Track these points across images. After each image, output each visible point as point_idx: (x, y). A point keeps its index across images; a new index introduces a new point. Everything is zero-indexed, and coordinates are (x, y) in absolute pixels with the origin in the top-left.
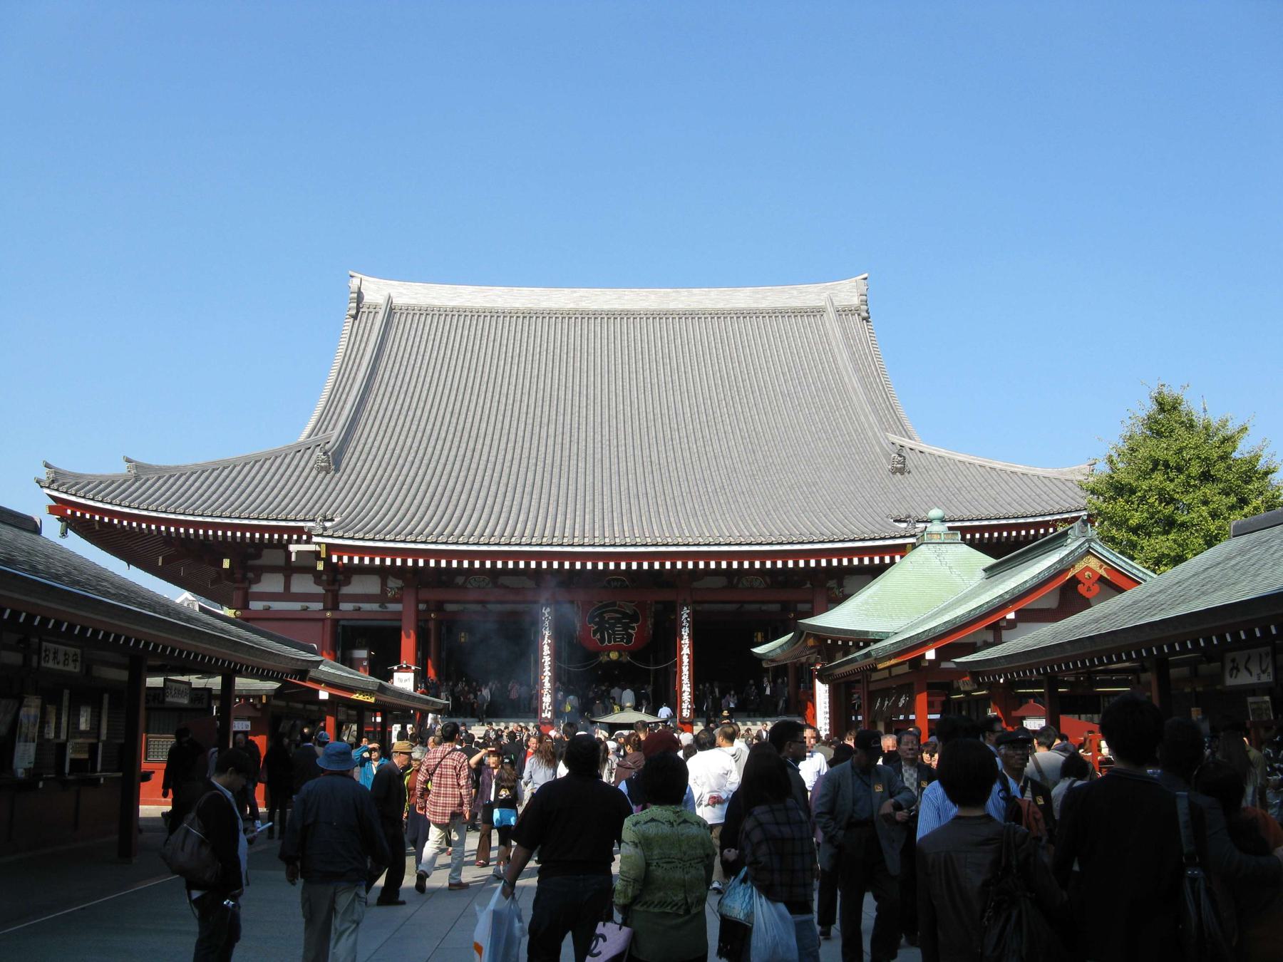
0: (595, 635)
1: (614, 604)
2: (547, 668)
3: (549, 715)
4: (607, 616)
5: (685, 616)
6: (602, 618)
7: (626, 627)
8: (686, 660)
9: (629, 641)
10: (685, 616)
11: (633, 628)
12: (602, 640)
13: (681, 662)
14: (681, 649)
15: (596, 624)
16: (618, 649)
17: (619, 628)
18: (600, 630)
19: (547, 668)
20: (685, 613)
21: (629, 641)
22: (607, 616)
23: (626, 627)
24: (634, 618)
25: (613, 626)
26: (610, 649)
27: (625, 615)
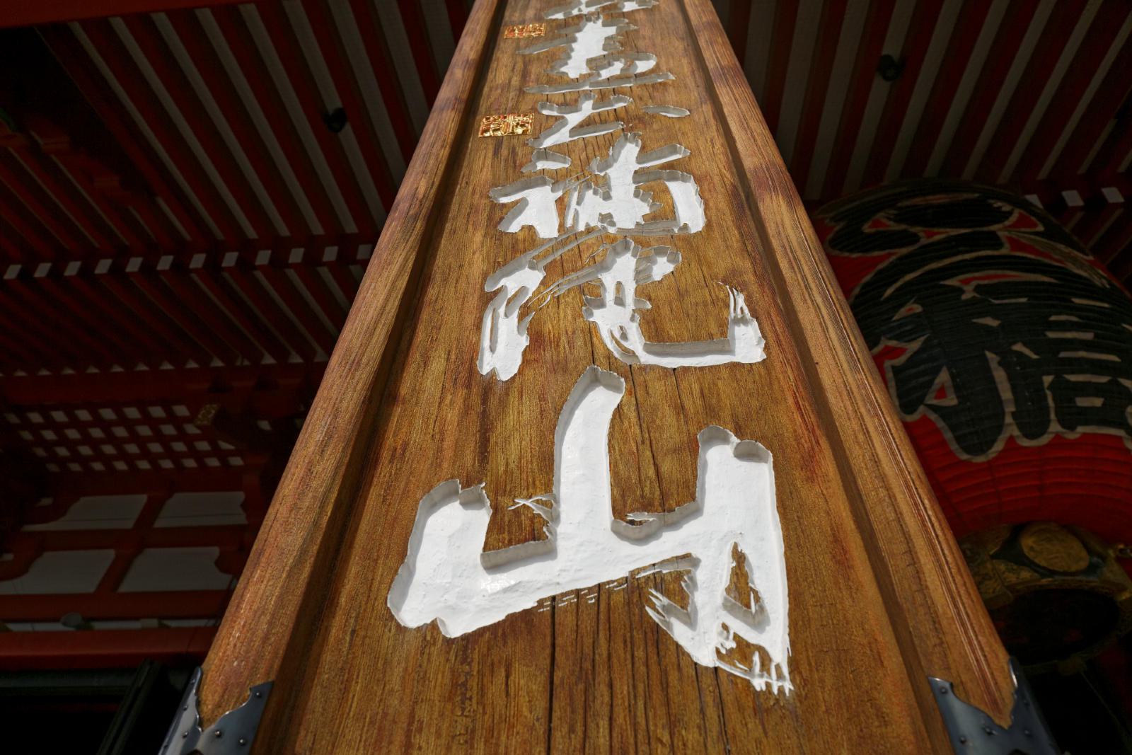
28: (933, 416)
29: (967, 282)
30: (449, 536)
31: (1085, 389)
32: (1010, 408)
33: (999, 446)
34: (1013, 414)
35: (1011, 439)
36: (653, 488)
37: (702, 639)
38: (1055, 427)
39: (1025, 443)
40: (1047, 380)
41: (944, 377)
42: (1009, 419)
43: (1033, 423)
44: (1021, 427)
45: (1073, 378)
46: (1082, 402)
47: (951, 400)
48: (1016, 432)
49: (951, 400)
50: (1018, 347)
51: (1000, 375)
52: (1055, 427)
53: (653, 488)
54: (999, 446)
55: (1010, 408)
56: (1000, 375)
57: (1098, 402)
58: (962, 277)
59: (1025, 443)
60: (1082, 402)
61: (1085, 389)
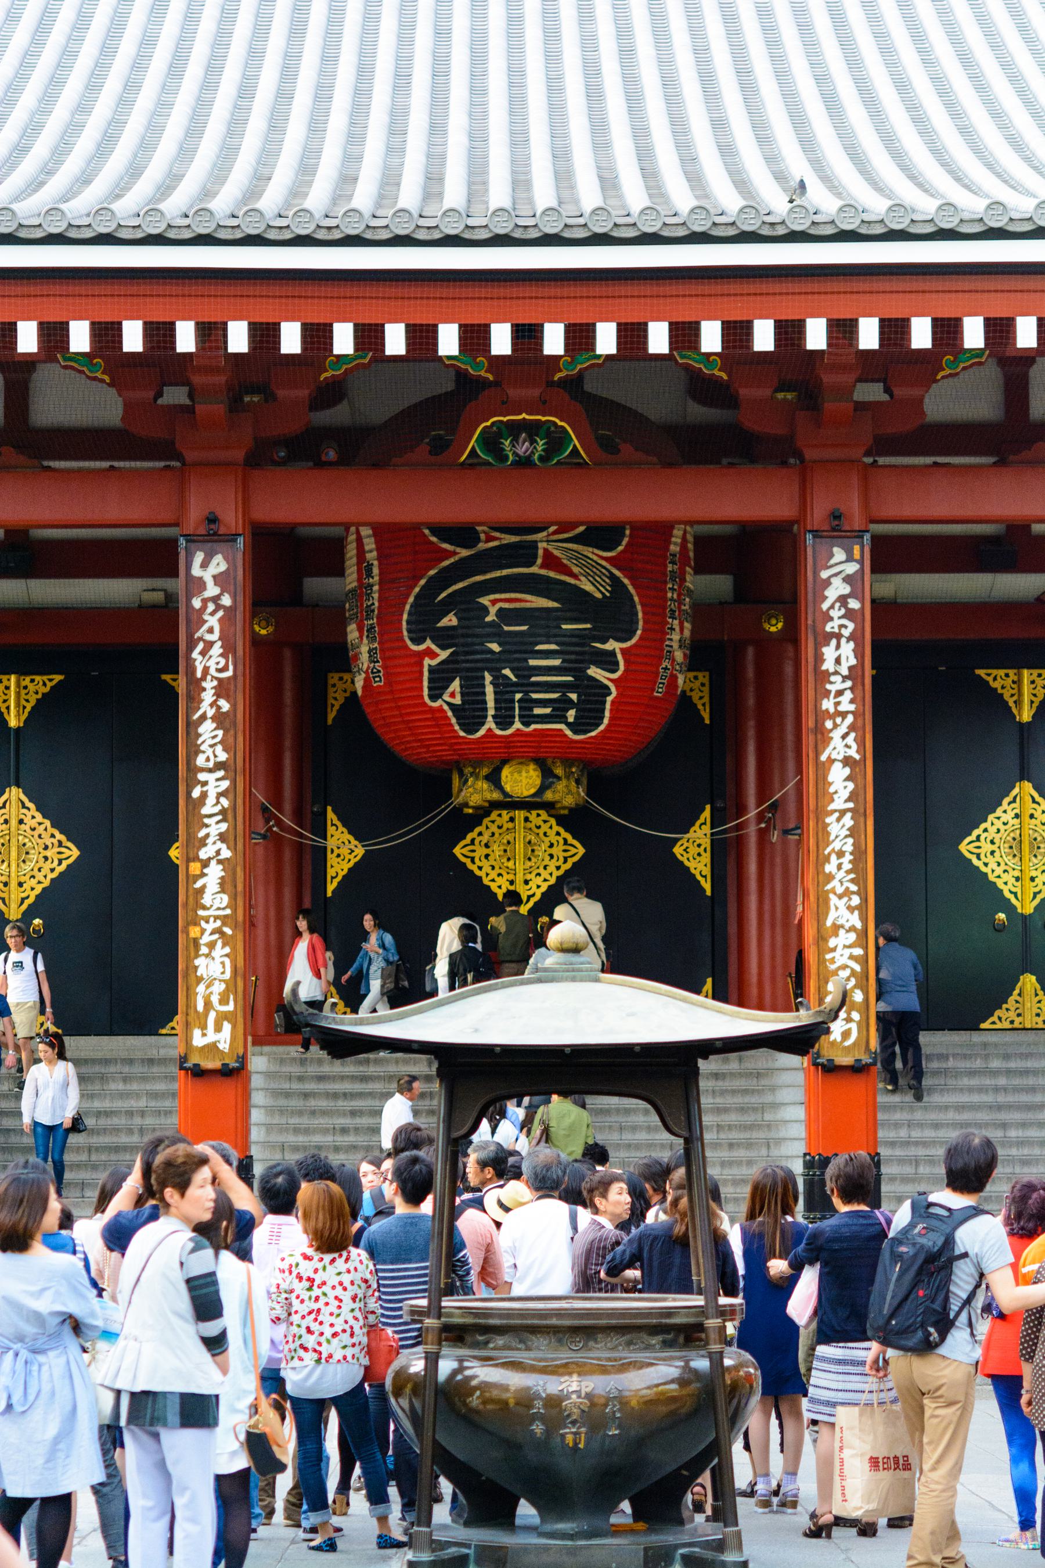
0: (440, 680)
1: (525, 554)
2: (215, 828)
3: (223, 1038)
4: (492, 605)
5: (838, 588)
6: (466, 604)
7: (580, 655)
8: (840, 783)
9: (588, 718)
10: (838, 588)
11: (608, 661)
12: (470, 713)
13: (824, 794)
14: (823, 738)
15: (444, 638)
16: (543, 755)
17: (547, 659)
18: (465, 666)
19: (215, 828)
20: (838, 579)
21: (588, 718)
22: (492, 605)
23: (580, 655)
24: (611, 614)
25: (518, 651)
26: (505, 753)
27: (576, 602)
28: (446, 707)
29: (494, 602)
30: (197, 1033)
31: (543, 703)
32: (491, 712)
33: (482, 732)
34: (494, 717)
35: (490, 730)
36: (218, 1029)
37: (221, 1046)
38: (518, 725)
39: (499, 732)
40: (518, 696)
41: (456, 685)
42: (490, 719)
43: (504, 720)
44: (496, 723)
45: (535, 696)
46: (537, 711)
47: (458, 700)
48: (493, 726)
49: (458, 700)
50: (507, 672)
51: (489, 690)
52: (518, 725)
53: (218, 1029)
54: (482, 732)
55: (491, 712)
56: (489, 690)
57: (548, 711)
58: (492, 597)
59: (499, 732)
60: (537, 711)
61: (543, 703)
